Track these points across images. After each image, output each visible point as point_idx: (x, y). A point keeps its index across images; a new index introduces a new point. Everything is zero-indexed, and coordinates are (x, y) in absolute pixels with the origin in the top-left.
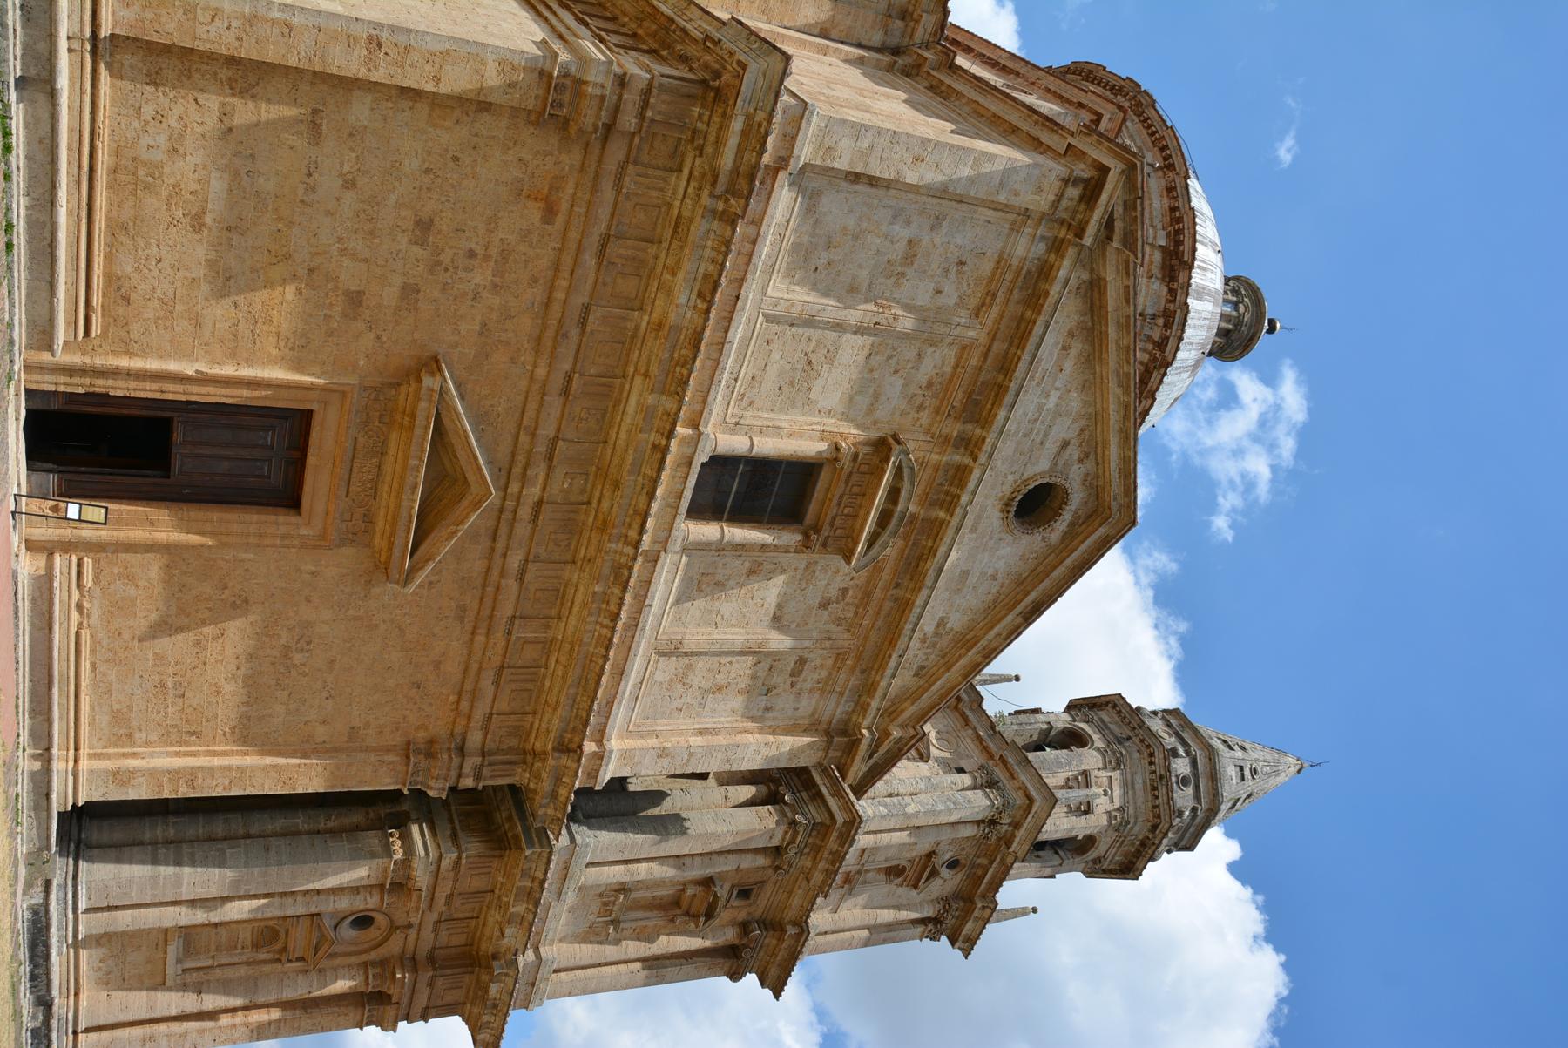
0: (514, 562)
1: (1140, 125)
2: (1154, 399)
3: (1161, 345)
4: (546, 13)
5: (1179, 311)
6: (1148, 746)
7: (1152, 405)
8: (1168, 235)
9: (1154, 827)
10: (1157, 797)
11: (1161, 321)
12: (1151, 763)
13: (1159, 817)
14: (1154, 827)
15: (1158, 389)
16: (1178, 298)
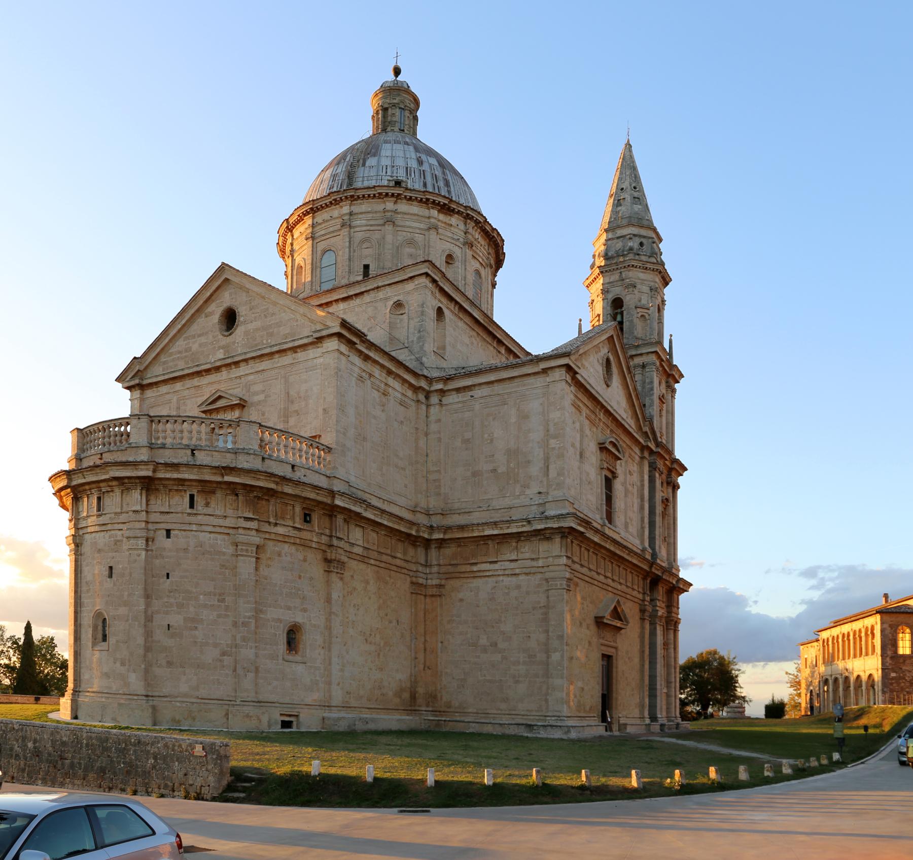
0: (619, 587)
1: (365, 201)
2: (495, 229)
3: (477, 222)
4: (485, 574)
5: (468, 212)
6: (629, 266)
7: (497, 230)
8: (433, 208)
9: (660, 272)
10: (650, 268)
11: (469, 221)
12: (636, 267)
13: (657, 269)
14: (660, 272)
15: (492, 226)
16: (462, 210)
